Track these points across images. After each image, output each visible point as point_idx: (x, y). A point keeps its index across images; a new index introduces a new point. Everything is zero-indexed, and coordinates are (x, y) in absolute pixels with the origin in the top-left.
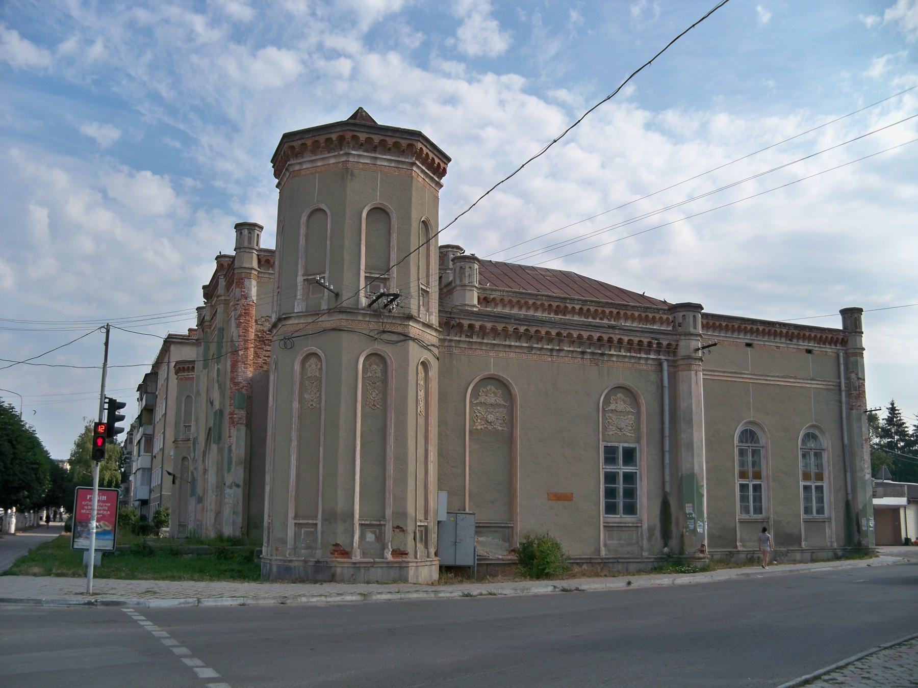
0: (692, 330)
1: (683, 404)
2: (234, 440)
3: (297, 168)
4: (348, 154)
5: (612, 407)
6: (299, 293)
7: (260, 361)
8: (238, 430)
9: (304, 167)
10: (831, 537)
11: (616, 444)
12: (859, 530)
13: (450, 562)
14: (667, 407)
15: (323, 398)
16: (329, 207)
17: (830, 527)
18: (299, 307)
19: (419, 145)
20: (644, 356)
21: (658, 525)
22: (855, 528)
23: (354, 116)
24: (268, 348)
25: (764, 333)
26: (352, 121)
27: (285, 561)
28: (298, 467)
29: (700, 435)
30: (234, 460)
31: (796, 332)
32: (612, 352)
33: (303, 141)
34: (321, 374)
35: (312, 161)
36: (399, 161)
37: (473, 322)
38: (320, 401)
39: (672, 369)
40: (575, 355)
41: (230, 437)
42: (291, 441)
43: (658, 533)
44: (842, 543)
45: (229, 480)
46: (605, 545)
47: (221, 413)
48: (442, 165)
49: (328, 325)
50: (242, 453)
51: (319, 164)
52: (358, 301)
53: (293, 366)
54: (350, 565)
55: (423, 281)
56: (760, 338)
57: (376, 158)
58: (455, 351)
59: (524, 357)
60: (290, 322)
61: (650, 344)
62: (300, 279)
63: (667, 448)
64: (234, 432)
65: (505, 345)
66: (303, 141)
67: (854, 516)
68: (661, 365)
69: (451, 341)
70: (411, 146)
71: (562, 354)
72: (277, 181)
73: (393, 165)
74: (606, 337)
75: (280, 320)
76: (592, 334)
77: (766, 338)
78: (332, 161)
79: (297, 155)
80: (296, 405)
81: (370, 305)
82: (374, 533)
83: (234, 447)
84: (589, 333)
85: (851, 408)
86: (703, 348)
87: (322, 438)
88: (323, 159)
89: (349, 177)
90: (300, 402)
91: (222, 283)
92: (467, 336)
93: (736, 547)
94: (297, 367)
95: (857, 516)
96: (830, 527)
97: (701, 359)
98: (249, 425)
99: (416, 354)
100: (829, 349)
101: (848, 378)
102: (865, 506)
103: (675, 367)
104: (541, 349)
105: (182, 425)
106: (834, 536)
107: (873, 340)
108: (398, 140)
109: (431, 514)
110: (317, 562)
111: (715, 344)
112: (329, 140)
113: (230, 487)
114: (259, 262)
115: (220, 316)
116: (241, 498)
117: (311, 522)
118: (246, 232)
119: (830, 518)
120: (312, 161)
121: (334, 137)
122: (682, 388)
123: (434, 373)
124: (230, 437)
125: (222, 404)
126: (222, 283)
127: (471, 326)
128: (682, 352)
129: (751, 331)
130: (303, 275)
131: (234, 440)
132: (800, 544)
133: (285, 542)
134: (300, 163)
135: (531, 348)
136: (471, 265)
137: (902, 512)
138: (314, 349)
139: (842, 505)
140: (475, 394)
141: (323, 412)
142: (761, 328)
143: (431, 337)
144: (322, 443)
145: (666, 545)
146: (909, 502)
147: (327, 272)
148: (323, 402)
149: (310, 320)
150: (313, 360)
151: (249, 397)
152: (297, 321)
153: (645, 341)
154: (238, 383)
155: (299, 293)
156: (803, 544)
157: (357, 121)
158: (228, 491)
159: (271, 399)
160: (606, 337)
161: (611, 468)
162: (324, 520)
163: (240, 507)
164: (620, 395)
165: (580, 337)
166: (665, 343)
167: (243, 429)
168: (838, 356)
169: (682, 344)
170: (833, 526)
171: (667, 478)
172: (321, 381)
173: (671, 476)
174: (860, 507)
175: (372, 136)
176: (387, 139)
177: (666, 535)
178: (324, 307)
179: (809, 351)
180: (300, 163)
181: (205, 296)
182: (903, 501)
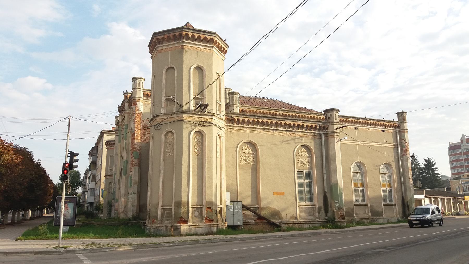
0: (335, 120)
1: (331, 153)
2: (133, 173)
3: (160, 48)
5: (300, 154)
6: (163, 104)
7: (145, 138)
8: (135, 168)
10: (396, 213)
11: (302, 170)
12: (408, 210)
13: (232, 224)
14: (324, 154)
15: (175, 151)
16: (175, 66)
17: (395, 208)
18: (163, 111)
19: (215, 39)
20: (313, 131)
21: (323, 207)
22: (407, 208)
23: (186, 25)
24: (149, 132)
25: (363, 123)
26: (185, 27)
27: (157, 227)
28: (163, 183)
29: (339, 166)
30: (133, 182)
31: (377, 122)
32: (299, 130)
33: (162, 36)
34: (174, 140)
35: (167, 45)
36: (206, 46)
37: (240, 118)
38: (173, 151)
39: (326, 138)
40: (284, 132)
42: (160, 171)
43: (323, 210)
44: (401, 215)
45: (130, 191)
46: (300, 216)
47: (127, 161)
48: (225, 49)
49: (176, 119)
50: (137, 178)
51: (170, 47)
52: (189, 108)
53: (161, 137)
54: (187, 227)
55: (218, 99)
56: (361, 125)
57: (196, 44)
58: (233, 130)
59: (262, 133)
60: (159, 118)
61: (316, 126)
62: (163, 98)
63: (325, 172)
64: (133, 169)
65: (253, 128)
66: (162, 36)
67: (406, 203)
68: (321, 136)
69: (230, 126)
70: (212, 39)
71: (277, 131)
72: (151, 55)
73: (204, 47)
74: (296, 124)
75: (154, 117)
76: (291, 122)
77: (363, 126)
78: (176, 45)
79: (160, 42)
80: (162, 154)
81: (195, 110)
82: (198, 211)
83: (133, 177)
84: (289, 122)
85: (402, 156)
86: (340, 128)
87: (174, 169)
88: (172, 44)
89: (184, 53)
90: (164, 153)
91: (127, 104)
92: (237, 124)
93: (354, 217)
94: (163, 138)
95: (407, 202)
96: (395, 208)
97: (339, 133)
98: (140, 166)
99: (215, 131)
100: (392, 130)
101: (401, 142)
102: (411, 199)
103: (327, 136)
104: (269, 129)
105: (109, 168)
106: (397, 212)
107: (411, 126)
108: (206, 36)
109: (223, 202)
111: (346, 126)
112: (175, 36)
113: (131, 194)
114: (144, 94)
115: (126, 119)
116: (136, 199)
117: (169, 207)
118: (137, 81)
119: (395, 205)
120: (167, 45)
121: (177, 34)
122: (331, 146)
123: (223, 140)
125: (127, 157)
126: (127, 104)
127: (239, 120)
128: (330, 130)
129: (357, 123)
130: (165, 97)
131: (133, 173)
132: (382, 216)
133: (157, 218)
134: (162, 46)
135: (265, 129)
136: (236, 96)
137: (423, 201)
138: (171, 130)
139: (401, 198)
140: (242, 148)
141: (175, 157)
142: (361, 121)
143: (222, 123)
144: (174, 172)
145: (326, 215)
146: (426, 197)
147: (176, 95)
148: (175, 153)
149: (168, 116)
150: (170, 134)
151: (140, 154)
152: (162, 117)
153: (314, 125)
154: (135, 148)
155: (163, 104)
156: (384, 215)
157: (187, 27)
158: (130, 196)
159: (150, 153)
160: (296, 124)
161: (301, 181)
162: (175, 206)
163: (136, 204)
164: (303, 149)
165: (285, 124)
166: (322, 126)
167: (137, 168)
168: (396, 133)
169: (330, 126)
170: (397, 208)
171: (325, 185)
172: (174, 144)
173: (327, 184)
174: (409, 199)
175: (194, 34)
176: (201, 35)
177: (326, 211)
178: (174, 111)
179: (383, 131)
180: (162, 46)
181: (119, 111)
182: (422, 197)
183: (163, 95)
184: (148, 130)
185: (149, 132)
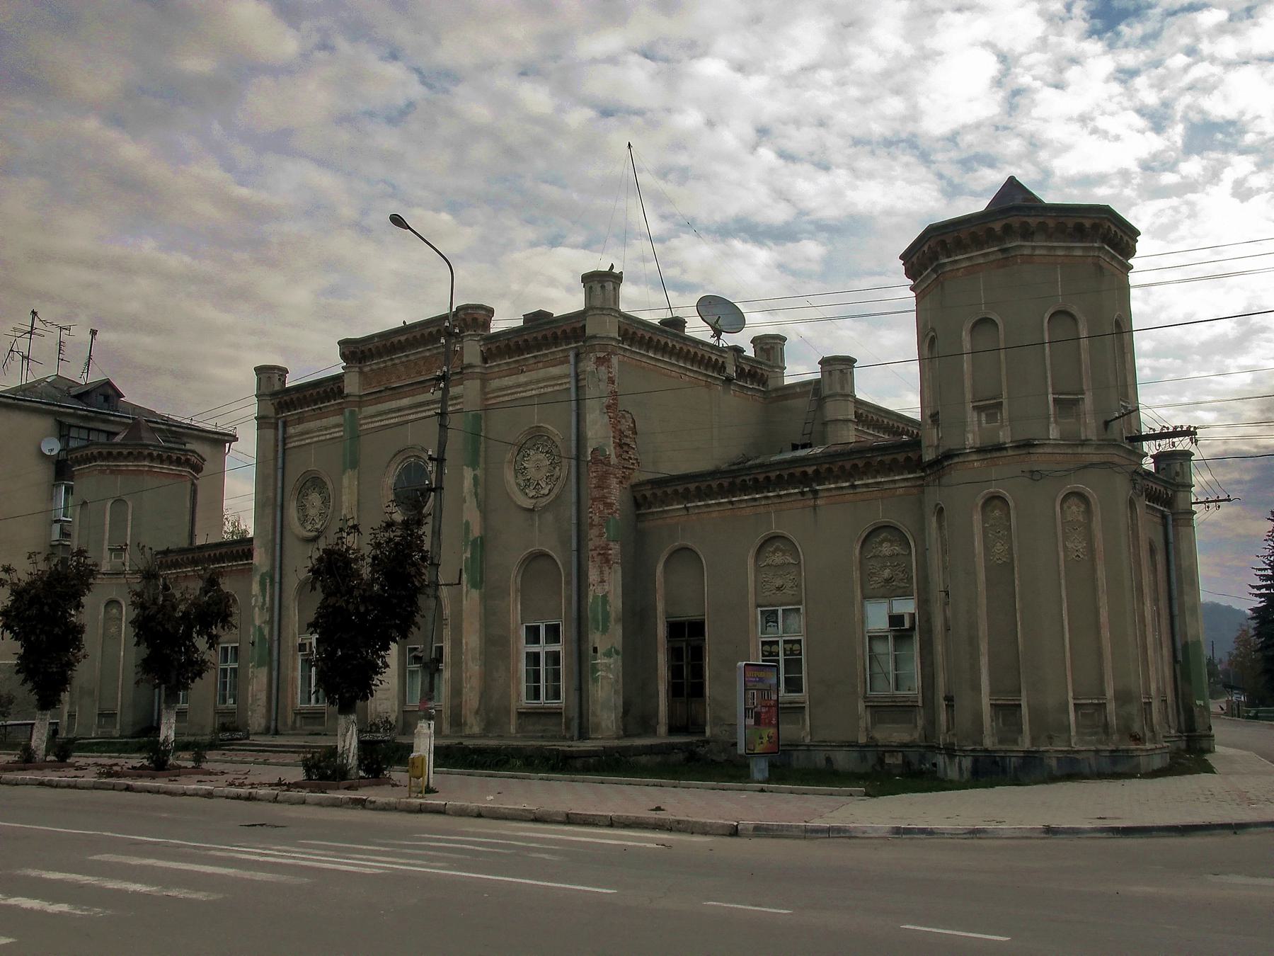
4: (1100, 249)
9: (1037, 252)
24: (625, 456)
30: (613, 616)
41: (603, 581)
49: (1095, 459)
83: (611, 598)
105: (106, 547)
110: (1112, 751)
113: (608, 654)
118: (609, 286)
124: (603, 581)
150: (1074, 500)
167: (618, 568)
183: (1050, 390)
184: (626, 448)
185: (625, 456)
